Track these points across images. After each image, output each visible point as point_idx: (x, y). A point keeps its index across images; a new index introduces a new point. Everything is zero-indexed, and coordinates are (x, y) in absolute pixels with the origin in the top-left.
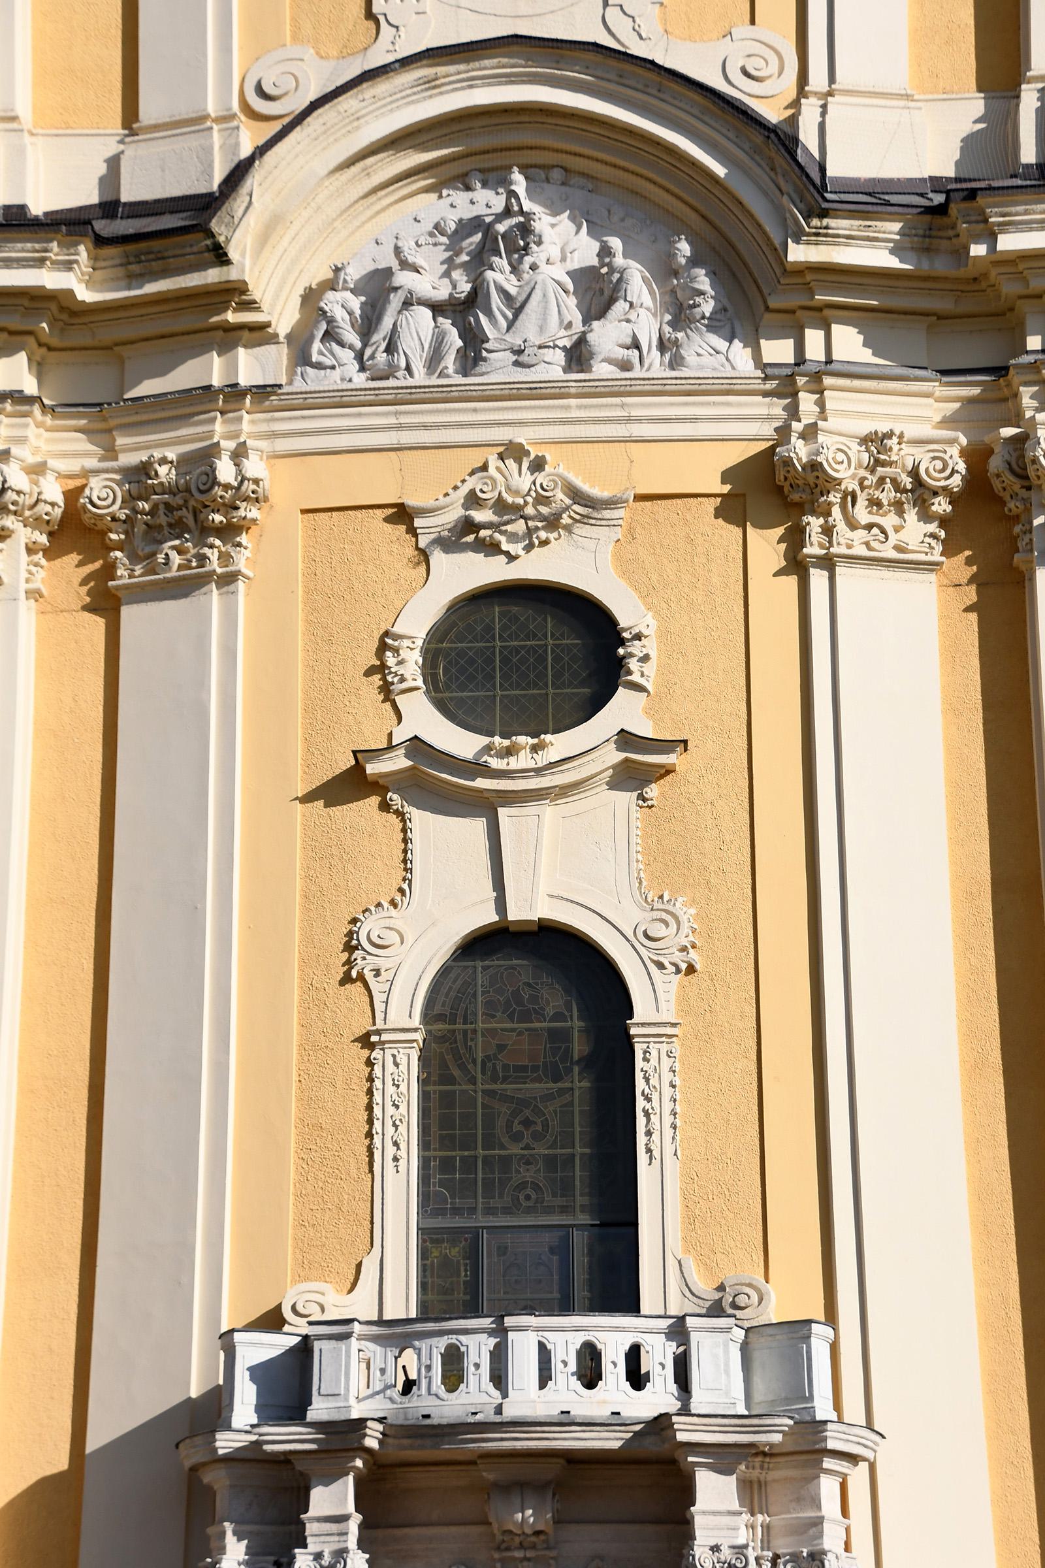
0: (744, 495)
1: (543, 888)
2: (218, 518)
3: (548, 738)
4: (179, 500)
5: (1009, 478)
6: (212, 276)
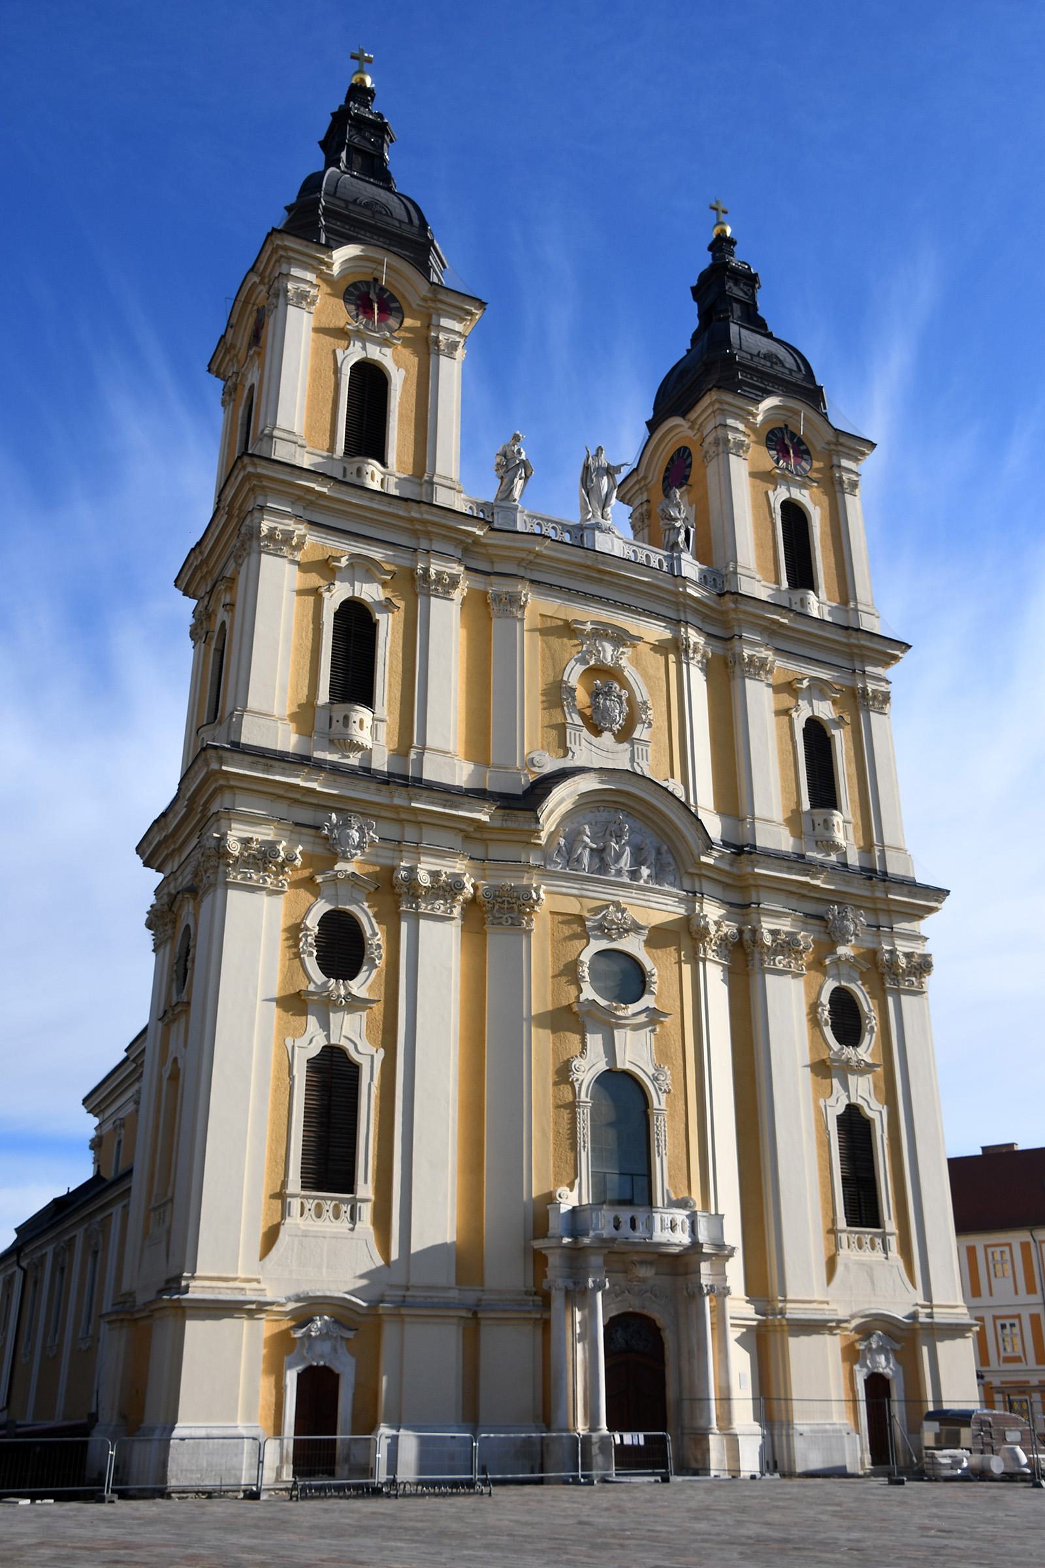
4: (514, 900)
5: (750, 942)
6: (533, 827)
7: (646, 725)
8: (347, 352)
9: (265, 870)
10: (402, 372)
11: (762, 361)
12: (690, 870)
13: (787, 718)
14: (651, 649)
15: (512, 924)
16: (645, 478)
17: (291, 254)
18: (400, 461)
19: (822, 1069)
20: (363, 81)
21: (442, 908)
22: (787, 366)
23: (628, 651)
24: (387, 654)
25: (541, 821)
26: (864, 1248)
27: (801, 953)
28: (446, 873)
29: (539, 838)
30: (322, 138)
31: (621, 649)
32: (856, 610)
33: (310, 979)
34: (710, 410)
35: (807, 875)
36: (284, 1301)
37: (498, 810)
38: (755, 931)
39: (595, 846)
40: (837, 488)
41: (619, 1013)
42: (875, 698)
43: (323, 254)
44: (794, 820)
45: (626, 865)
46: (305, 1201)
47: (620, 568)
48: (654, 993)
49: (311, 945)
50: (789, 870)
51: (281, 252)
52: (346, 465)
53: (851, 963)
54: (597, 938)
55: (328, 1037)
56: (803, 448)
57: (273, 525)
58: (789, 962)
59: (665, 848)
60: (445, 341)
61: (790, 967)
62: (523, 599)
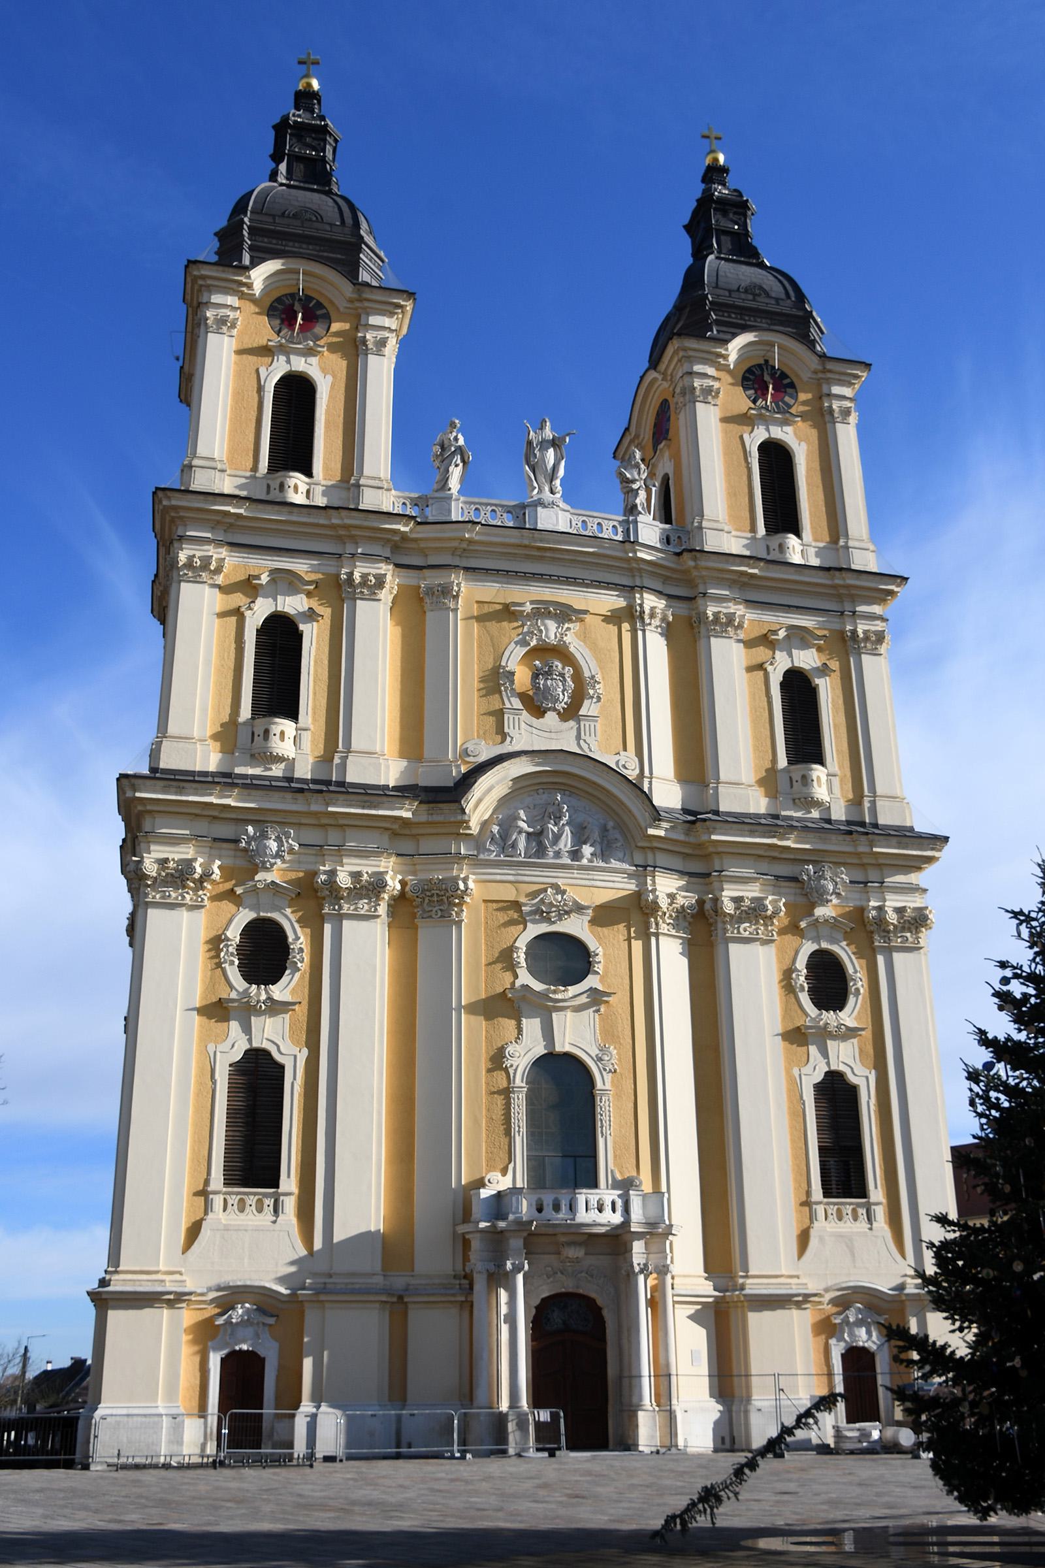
0: (629, 909)
1: (567, 1040)
2: (457, 901)
3: (569, 988)
4: (442, 893)
6: (459, 818)
7: (595, 700)
8: (270, 369)
9: (184, 887)
10: (329, 378)
11: (743, 296)
12: (639, 844)
13: (761, 673)
14: (603, 621)
15: (442, 917)
16: (637, 436)
17: (209, 282)
18: (326, 468)
19: (796, 1036)
20: (309, 85)
21: (366, 907)
22: (773, 295)
23: (575, 627)
24: (312, 663)
25: (467, 811)
26: (844, 1219)
27: (771, 918)
28: (367, 873)
29: (469, 828)
30: (271, 152)
31: (566, 625)
32: (847, 547)
33: (232, 987)
34: (676, 359)
35: (774, 837)
36: (205, 1291)
37: (422, 805)
38: (716, 901)
39: (531, 830)
40: (827, 418)
41: (559, 996)
42: (867, 638)
43: (241, 275)
44: (769, 781)
45: (565, 846)
46: (228, 1197)
47: (559, 543)
48: (598, 973)
49: (232, 954)
50: (752, 833)
51: (201, 282)
52: (270, 482)
53: (833, 924)
54: (534, 922)
55: (250, 1041)
56: (786, 381)
57: (191, 553)
58: (757, 929)
59: (611, 824)
60: (372, 340)
61: (758, 934)
62: (456, 588)
